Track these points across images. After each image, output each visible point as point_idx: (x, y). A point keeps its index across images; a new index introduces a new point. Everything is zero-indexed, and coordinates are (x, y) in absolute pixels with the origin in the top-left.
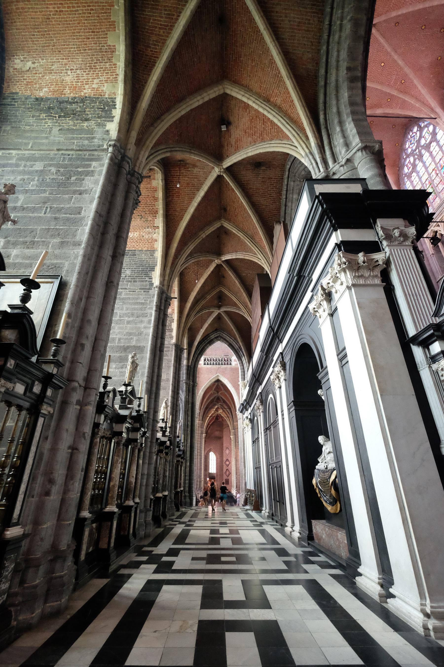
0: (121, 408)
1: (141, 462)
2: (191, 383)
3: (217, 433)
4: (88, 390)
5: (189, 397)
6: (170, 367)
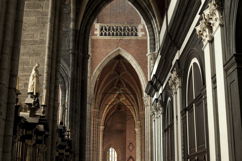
2: (81, 54)
3: (118, 126)
5: (77, 73)
6: (46, 23)
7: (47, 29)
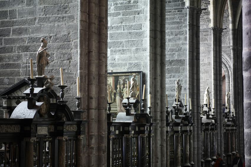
0: (176, 118)
1: (192, 141)
4: (162, 121)
5: (238, 64)
7: (211, 55)
